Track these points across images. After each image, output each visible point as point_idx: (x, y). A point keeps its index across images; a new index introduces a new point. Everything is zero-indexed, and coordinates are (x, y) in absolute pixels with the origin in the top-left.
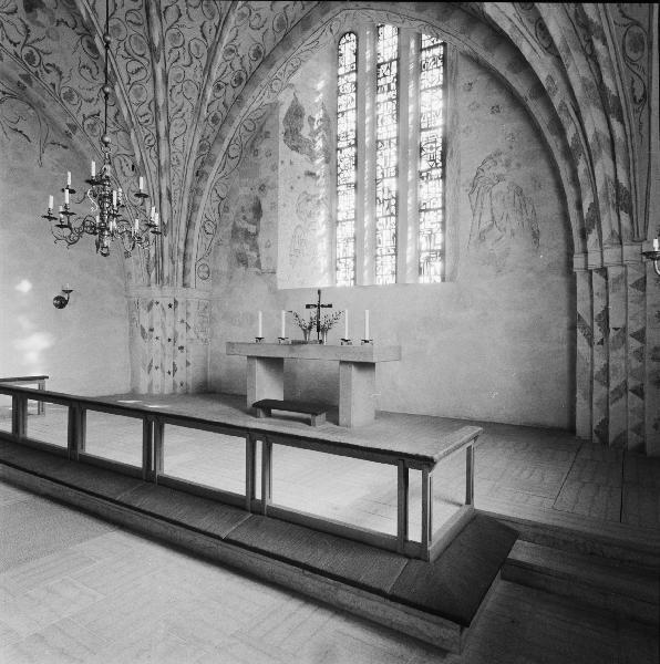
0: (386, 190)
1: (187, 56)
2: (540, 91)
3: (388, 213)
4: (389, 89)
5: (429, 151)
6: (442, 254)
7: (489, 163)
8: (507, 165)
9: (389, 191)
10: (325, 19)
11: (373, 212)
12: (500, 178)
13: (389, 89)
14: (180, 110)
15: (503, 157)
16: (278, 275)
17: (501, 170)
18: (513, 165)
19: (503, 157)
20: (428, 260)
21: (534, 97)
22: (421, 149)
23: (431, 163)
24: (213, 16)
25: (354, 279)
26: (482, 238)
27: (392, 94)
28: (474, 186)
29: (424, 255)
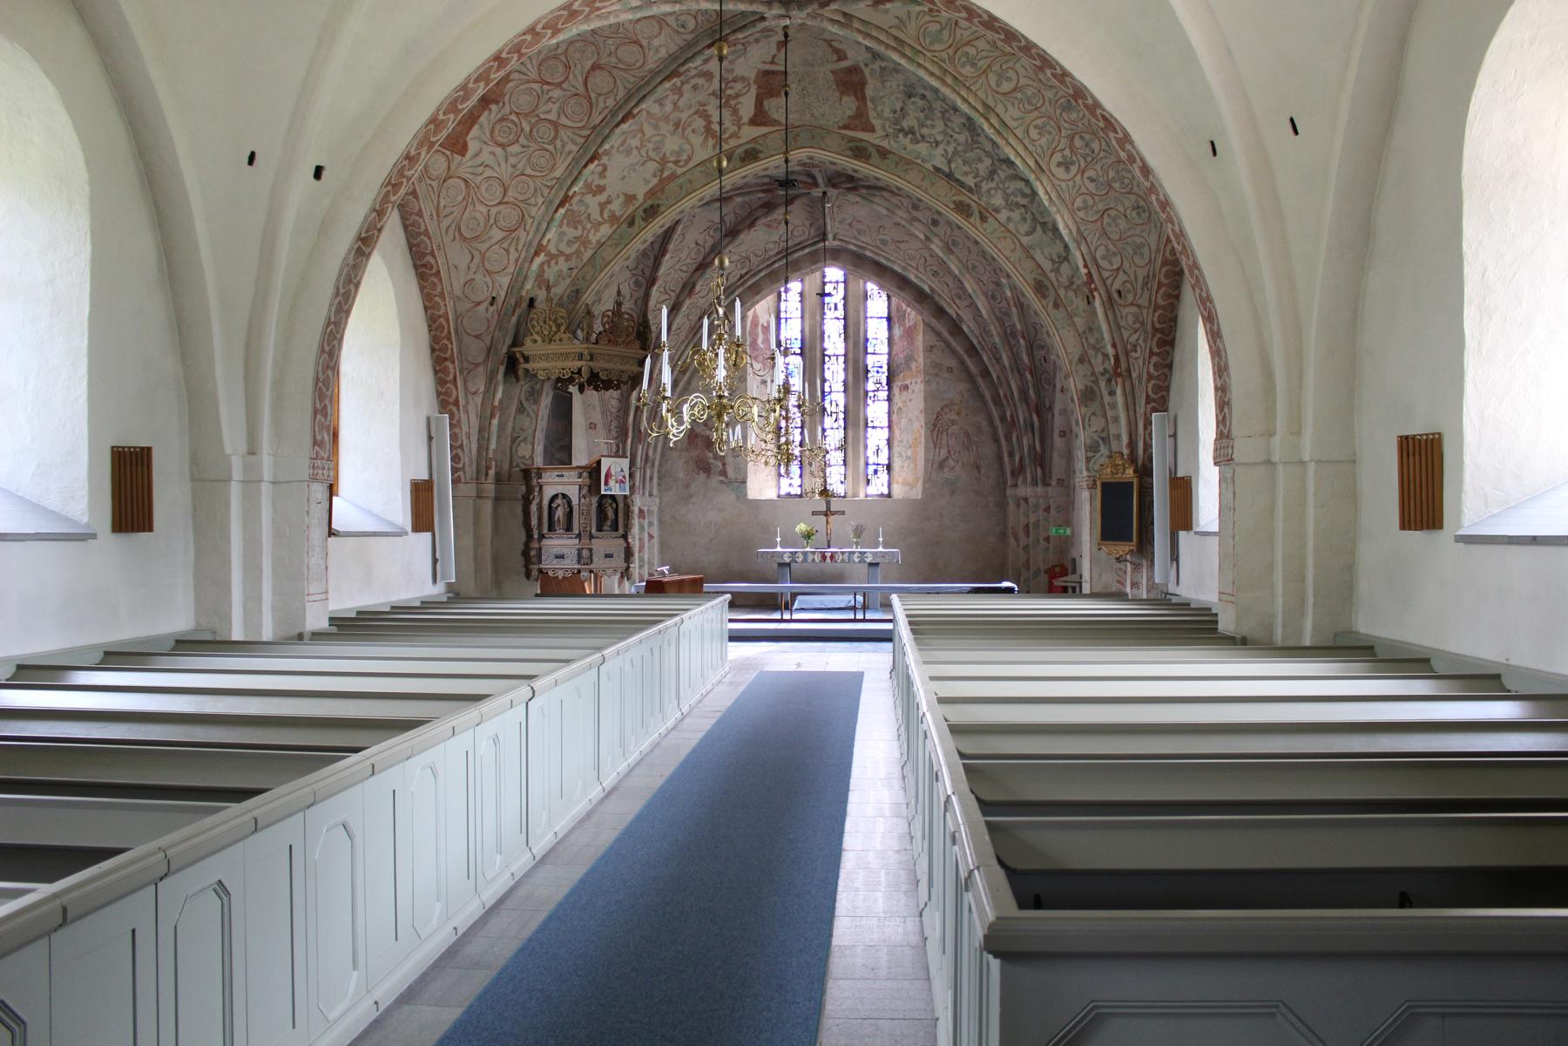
0: (834, 404)
1: (706, 292)
2: (986, 373)
3: (836, 425)
4: (836, 309)
5: (875, 374)
6: (889, 467)
7: (946, 410)
8: (958, 413)
9: (837, 405)
10: (814, 267)
11: (822, 423)
12: (953, 422)
13: (836, 309)
14: (679, 329)
15: (956, 408)
16: (749, 484)
17: (953, 416)
18: (963, 414)
19: (956, 408)
20: (876, 472)
21: (983, 377)
22: (868, 371)
23: (878, 386)
24: (742, 269)
25: (801, 486)
26: (941, 466)
27: (840, 313)
28: (935, 426)
29: (871, 469)
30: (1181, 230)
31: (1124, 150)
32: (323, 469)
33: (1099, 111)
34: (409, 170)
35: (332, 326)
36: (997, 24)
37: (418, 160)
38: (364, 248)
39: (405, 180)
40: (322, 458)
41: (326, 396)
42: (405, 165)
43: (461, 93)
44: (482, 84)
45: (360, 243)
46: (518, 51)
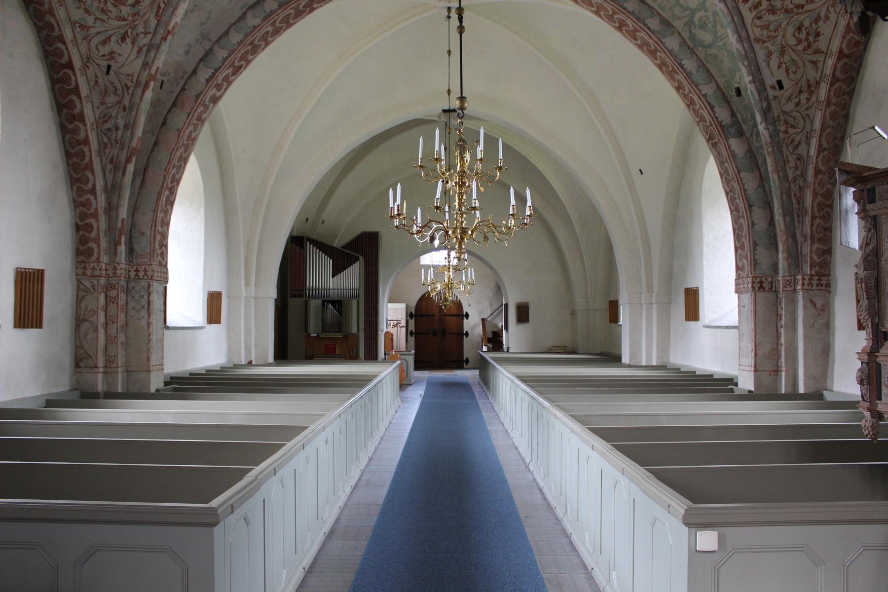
30: (194, 139)
31: (223, 80)
32: (744, 284)
33: (243, 63)
34: (685, 90)
35: (730, 194)
36: (308, 10)
37: (681, 82)
38: (714, 141)
39: (690, 95)
40: (743, 277)
41: (742, 236)
42: (682, 93)
43: (645, 48)
44: (638, 34)
45: (710, 142)
46: (612, 16)
